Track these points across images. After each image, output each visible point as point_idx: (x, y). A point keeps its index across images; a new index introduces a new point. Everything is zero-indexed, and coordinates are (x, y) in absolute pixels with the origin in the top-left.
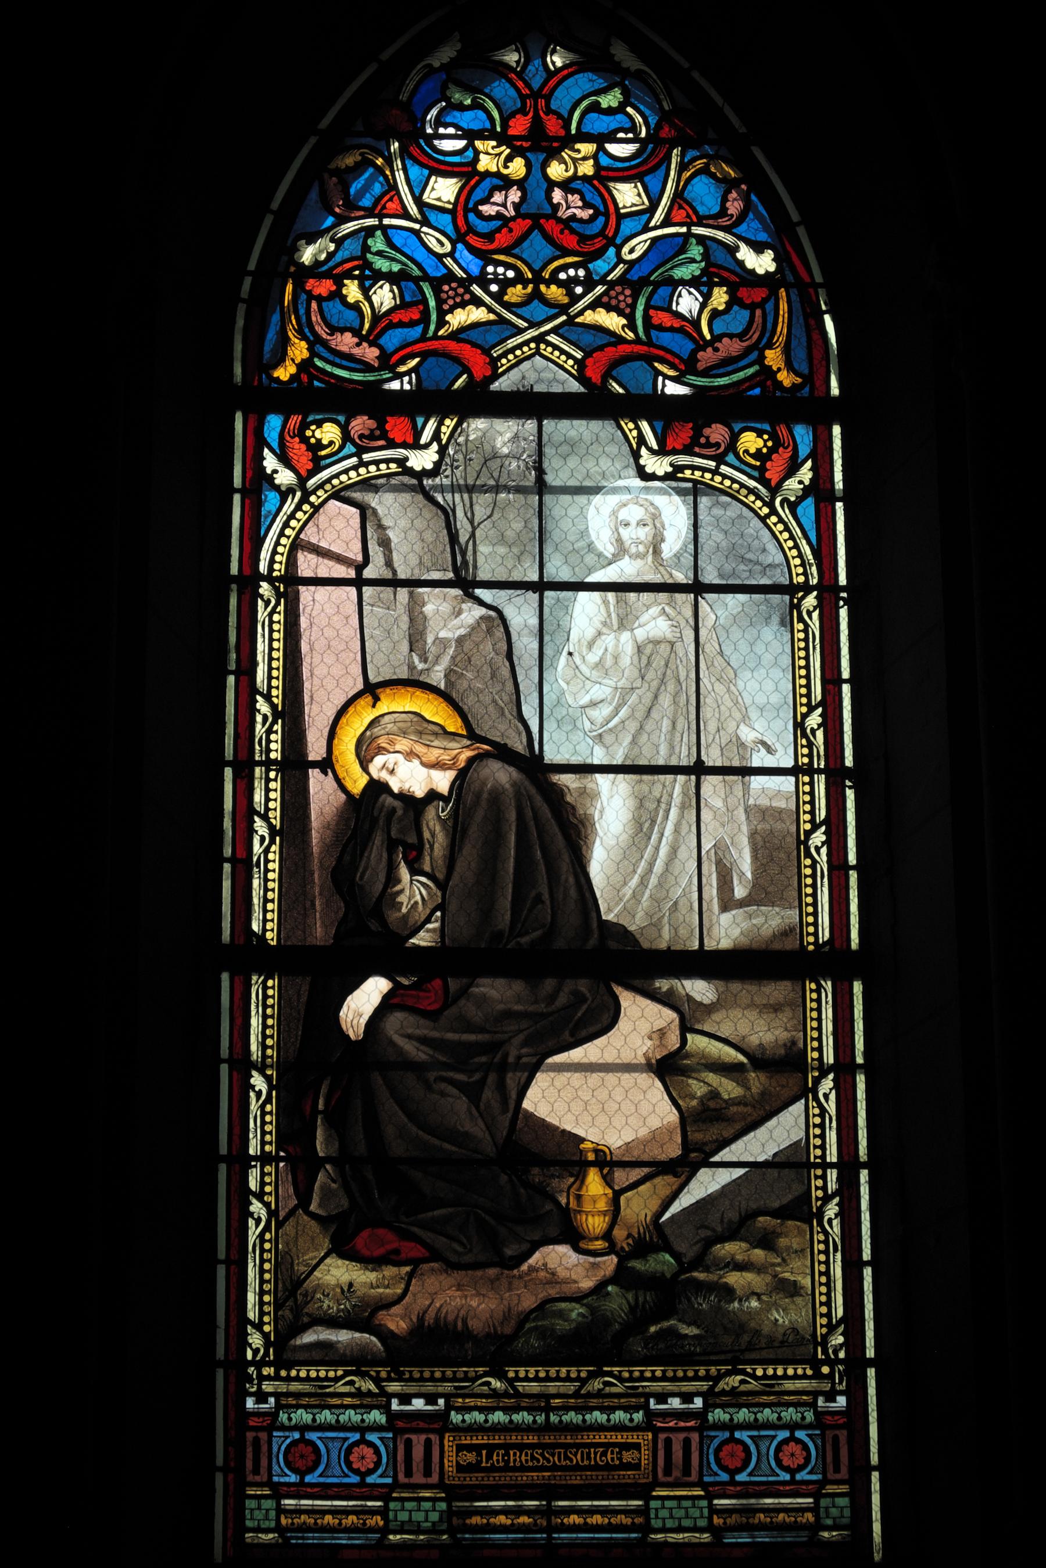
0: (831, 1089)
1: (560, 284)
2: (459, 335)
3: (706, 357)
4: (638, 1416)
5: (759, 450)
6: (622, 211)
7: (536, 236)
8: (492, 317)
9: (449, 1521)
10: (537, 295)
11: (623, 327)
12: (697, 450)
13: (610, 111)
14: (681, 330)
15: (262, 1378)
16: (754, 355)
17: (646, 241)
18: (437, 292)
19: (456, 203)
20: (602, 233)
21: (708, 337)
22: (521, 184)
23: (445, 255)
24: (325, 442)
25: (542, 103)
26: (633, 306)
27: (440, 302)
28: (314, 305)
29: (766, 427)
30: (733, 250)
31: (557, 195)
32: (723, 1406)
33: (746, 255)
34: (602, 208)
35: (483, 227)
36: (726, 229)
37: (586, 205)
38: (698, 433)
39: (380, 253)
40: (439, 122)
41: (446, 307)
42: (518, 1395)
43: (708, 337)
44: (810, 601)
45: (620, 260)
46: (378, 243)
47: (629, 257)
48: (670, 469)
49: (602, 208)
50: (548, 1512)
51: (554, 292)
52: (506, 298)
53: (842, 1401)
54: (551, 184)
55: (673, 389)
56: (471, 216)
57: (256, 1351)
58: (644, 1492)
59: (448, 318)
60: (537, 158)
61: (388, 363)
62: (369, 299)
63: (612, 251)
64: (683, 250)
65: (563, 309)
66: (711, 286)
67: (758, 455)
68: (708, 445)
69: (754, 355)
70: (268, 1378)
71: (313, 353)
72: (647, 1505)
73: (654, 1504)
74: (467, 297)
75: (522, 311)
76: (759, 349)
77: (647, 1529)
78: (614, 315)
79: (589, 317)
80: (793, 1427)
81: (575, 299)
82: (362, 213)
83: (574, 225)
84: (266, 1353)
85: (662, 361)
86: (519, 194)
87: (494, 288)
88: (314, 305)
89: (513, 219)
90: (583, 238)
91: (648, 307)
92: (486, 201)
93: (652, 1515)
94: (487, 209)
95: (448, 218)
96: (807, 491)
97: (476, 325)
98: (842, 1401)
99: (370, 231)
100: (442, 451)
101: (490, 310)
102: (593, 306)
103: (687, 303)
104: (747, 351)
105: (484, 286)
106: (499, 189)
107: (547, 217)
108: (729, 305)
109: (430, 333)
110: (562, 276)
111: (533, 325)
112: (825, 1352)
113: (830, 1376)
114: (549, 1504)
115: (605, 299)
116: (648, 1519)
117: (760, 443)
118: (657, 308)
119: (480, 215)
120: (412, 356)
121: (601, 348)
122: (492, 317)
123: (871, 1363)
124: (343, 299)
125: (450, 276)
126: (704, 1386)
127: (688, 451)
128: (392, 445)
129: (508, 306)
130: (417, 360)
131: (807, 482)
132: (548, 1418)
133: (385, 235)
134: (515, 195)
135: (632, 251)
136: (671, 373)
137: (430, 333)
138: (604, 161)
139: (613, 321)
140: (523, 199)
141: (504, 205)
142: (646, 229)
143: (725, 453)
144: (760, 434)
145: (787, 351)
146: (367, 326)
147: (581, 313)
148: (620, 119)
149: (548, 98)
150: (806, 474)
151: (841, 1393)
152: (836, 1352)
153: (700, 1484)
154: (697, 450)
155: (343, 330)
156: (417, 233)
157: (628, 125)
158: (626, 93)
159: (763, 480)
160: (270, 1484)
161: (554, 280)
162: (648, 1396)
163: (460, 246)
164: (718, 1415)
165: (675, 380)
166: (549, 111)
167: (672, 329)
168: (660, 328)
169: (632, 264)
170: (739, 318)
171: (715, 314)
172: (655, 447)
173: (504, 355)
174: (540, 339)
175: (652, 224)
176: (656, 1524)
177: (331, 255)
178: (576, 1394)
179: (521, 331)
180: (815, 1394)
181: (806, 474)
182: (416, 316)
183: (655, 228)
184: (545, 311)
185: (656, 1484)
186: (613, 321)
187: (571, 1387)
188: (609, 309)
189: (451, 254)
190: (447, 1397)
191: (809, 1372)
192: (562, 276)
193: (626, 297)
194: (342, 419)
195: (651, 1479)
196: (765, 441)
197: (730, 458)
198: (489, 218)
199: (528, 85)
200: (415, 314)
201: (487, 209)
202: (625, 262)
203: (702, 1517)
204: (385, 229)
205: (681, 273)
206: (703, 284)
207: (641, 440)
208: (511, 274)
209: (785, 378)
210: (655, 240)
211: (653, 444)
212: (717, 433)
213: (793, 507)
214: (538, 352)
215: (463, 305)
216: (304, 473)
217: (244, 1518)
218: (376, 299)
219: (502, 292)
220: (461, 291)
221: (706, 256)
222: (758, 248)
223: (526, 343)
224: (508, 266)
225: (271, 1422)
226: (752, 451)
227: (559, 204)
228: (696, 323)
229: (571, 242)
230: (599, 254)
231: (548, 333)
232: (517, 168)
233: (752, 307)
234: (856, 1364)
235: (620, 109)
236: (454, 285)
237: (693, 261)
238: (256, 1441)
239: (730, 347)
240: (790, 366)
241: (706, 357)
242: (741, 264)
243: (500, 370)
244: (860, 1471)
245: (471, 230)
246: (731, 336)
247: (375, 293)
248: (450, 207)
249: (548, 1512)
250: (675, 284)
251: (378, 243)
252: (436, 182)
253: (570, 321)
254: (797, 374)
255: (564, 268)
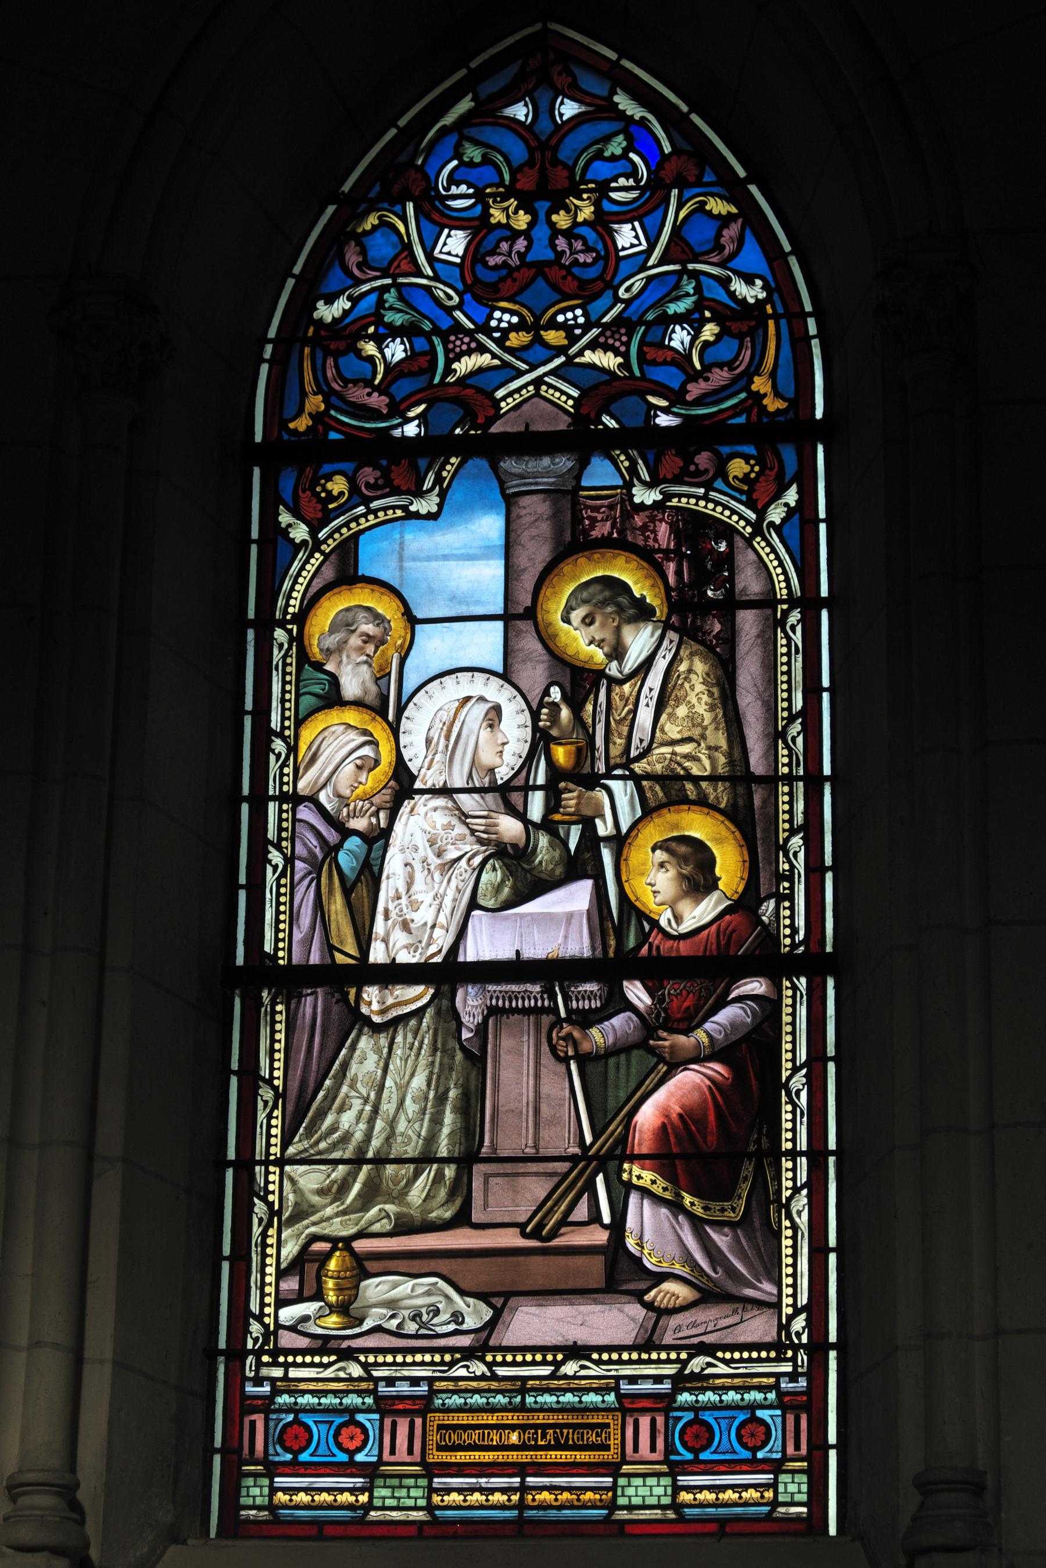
0: (803, 1085)
1: (558, 327)
2: (462, 380)
3: (695, 390)
4: (611, 1398)
5: (747, 475)
6: (622, 254)
7: (540, 283)
8: (496, 362)
9: (429, 1498)
10: (538, 340)
11: (620, 365)
12: (686, 479)
13: (613, 158)
14: (673, 363)
15: (260, 1364)
16: (743, 383)
17: (642, 279)
18: (445, 343)
19: (463, 258)
20: (600, 277)
21: (698, 366)
22: (527, 234)
23: (454, 308)
24: (335, 493)
25: (548, 154)
26: (627, 345)
27: (447, 352)
28: (330, 361)
29: (751, 450)
30: (725, 282)
31: (561, 243)
32: (689, 1390)
33: (739, 287)
34: (602, 253)
35: (490, 277)
36: (721, 265)
37: (588, 249)
38: (689, 460)
39: (391, 308)
40: (452, 180)
41: (451, 356)
42: (494, 1377)
43: (698, 366)
44: (795, 617)
45: (617, 300)
46: (391, 297)
47: (626, 296)
48: (660, 497)
49: (602, 253)
50: (523, 1489)
51: (554, 337)
52: (508, 344)
53: (803, 1383)
54: (555, 232)
55: (664, 420)
56: (479, 269)
57: (256, 1340)
58: (613, 1469)
59: (455, 366)
60: (542, 206)
61: (398, 411)
62: (382, 352)
63: (609, 293)
64: (677, 286)
65: (561, 350)
66: (704, 321)
67: (746, 479)
68: (699, 473)
69: (743, 383)
70: (268, 1364)
71: (329, 406)
72: (615, 1482)
73: (622, 1481)
74: (473, 345)
75: (524, 355)
76: (749, 375)
77: (613, 1506)
78: (610, 354)
79: (589, 357)
80: (753, 1407)
81: (573, 339)
82: (378, 274)
83: (575, 270)
84: (266, 1341)
85: (654, 394)
86: (525, 243)
87: (497, 335)
88: (330, 361)
89: (518, 268)
90: (583, 283)
91: (642, 343)
92: (493, 252)
93: (619, 1493)
94: (492, 261)
95: (458, 270)
96: (790, 512)
97: (481, 370)
98: (803, 1383)
99: (385, 289)
100: (443, 495)
101: (494, 356)
102: (593, 346)
103: (680, 338)
104: (735, 380)
105: (488, 331)
106: (506, 239)
107: (548, 264)
108: (719, 337)
109: (437, 380)
110: (560, 318)
111: (533, 368)
112: (789, 1336)
113: (794, 1359)
114: (523, 1482)
115: (602, 340)
116: (615, 1496)
117: (747, 469)
118: (650, 345)
119: (485, 264)
120: (418, 404)
121: (595, 387)
122: (496, 362)
123: (833, 1346)
124: (358, 353)
125: (458, 327)
126: (670, 1370)
127: (678, 480)
128: (396, 492)
129: (511, 351)
130: (423, 407)
131: (793, 504)
132: (523, 1399)
133: (399, 291)
134: (521, 244)
135: (627, 290)
136: (664, 403)
137: (437, 380)
138: (607, 206)
139: (609, 361)
140: (528, 248)
141: (509, 254)
142: (644, 268)
143: (714, 479)
144: (747, 458)
145: (773, 375)
146: (379, 377)
147: (581, 353)
148: (621, 166)
149: (556, 149)
150: (791, 496)
151: (802, 1374)
152: (798, 1335)
153: (666, 1461)
154: (686, 479)
155: (355, 382)
156: (427, 289)
157: (629, 169)
158: (628, 138)
159: (750, 504)
160: (266, 1462)
161: (553, 325)
162: (618, 1378)
163: (468, 297)
164: (685, 1398)
165: (666, 411)
166: (556, 162)
167: (665, 363)
168: (654, 363)
169: (628, 302)
170: (727, 349)
171: (706, 344)
172: (648, 479)
173: (504, 398)
174: (538, 382)
175: (650, 263)
176: (622, 1501)
177: (346, 313)
178: (553, 1376)
179: (521, 373)
180: (778, 1376)
181: (791, 496)
182: (425, 365)
183: (654, 267)
184: (544, 353)
185: (624, 1461)
186: (609, 361)
187: (546, 1371)
188: (606, 347)
189: (459, 307)
190: (431, 1380)
191: (773, 1354)
192: (560, 318)
193: (622, 335)
194: (349, 466)
195: (619, 1460)
196: (752, 467)
197: (719, 484)
198: (496, 267)
199: (536, 137)
200: (423, 362)
201: (492, 261)
202: (622, 301)
203: (666, 1495)
204: (399, 287)
205: (672, 308)
206: (693, 320)
207: (633, 470)
208: (515, 320)
209: (772, 404)
210: (650, 279)
211: (645, 475)
212: (703, 459)
213: (778, 529)
214: (537, 394)
215: (469, 353)
216: (315, 523)
217: (238, 1496)
218: (388, 352)
219: (505, 336)
220: (466, 340)
221: (698, 289)
222: (749, 280)
223: (525, 386)
224: (512, 313)
225: (266, 1405)
226: (741, 476)
227: (564, 252)
228: (688, 357)
229: (570, 286)
230: (597, 295)
231: (546, 374)
232: (522, 220)
233: (740, 337)
234: (818, 1348)
235: (624, 156)
236: (461, 336)
237: (688, 295)
238: (253, 1424)
239: (720, 377)
240: (777, 394)
241: (695, 390)
242: (732, 295)
243: (502, 411)
244: (819, 1446)
245: (476, 280)
246: (721, 366)
247: (387, 346)
248: (458, 260)
249: (523, 1489)
250: (667, 321)
251: (391, 297)
252: (449, 236)
253: (570, 360)
254: (784, 399)
255: (563, 311)
